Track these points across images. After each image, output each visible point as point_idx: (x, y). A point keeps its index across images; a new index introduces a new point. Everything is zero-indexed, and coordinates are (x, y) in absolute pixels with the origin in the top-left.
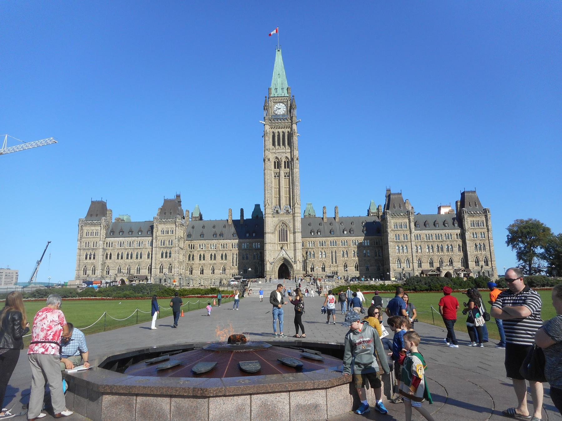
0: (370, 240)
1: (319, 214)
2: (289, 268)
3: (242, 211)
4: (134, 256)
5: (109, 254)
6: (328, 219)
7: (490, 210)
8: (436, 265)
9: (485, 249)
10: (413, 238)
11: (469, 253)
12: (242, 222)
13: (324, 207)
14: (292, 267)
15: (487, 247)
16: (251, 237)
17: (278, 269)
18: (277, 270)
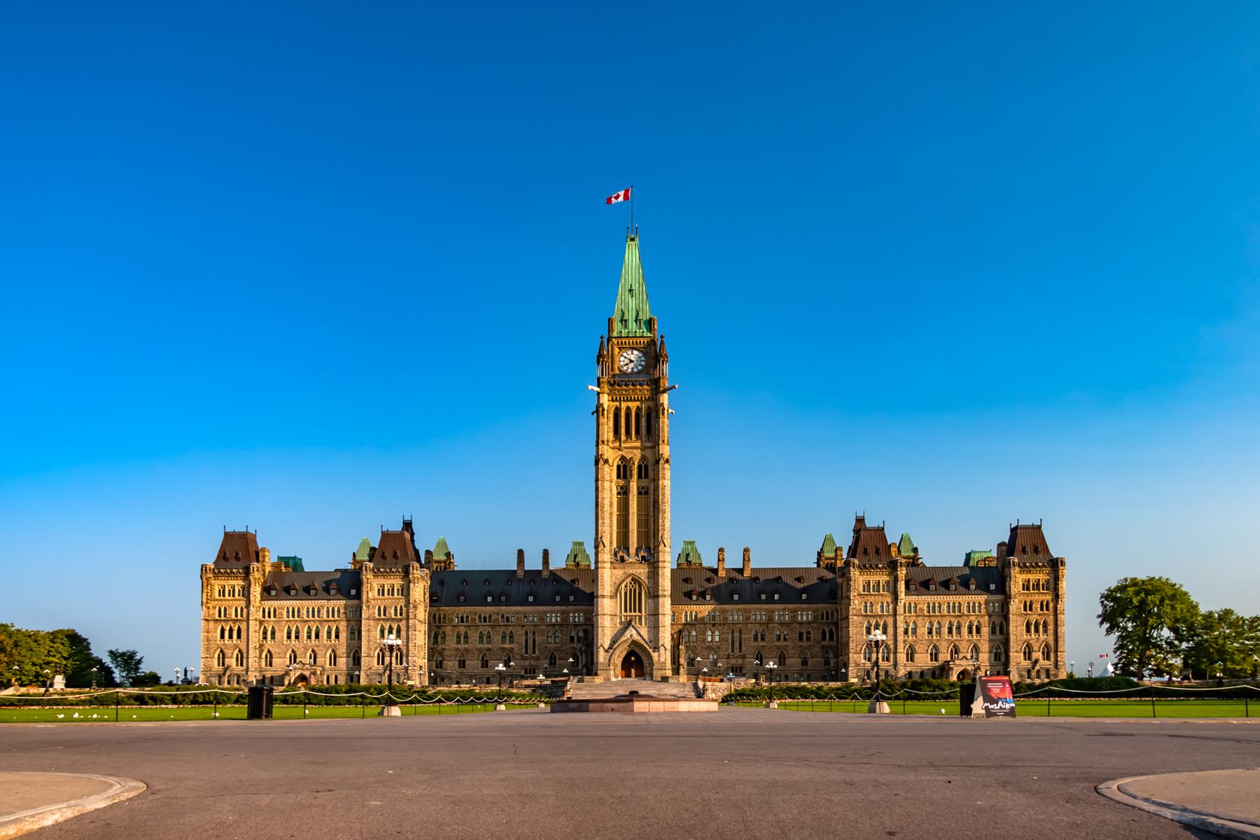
0: (815, 611)
1: (709, 561)
2: (644, 658)
3: (546, 553)
4: (324, 634)
5: (270, 629)
6: (728, 570)
7: (1066, 561)
8: (944, 656)
9: (1045, 631)
10: (900, 609)
11: (1012, 638)
12: (545, 574)
13: (721, 550)
14: (651, 658)
15: (1051, 627)
16: (564, 601)
17: (621, 659)
18: (618, 659)
